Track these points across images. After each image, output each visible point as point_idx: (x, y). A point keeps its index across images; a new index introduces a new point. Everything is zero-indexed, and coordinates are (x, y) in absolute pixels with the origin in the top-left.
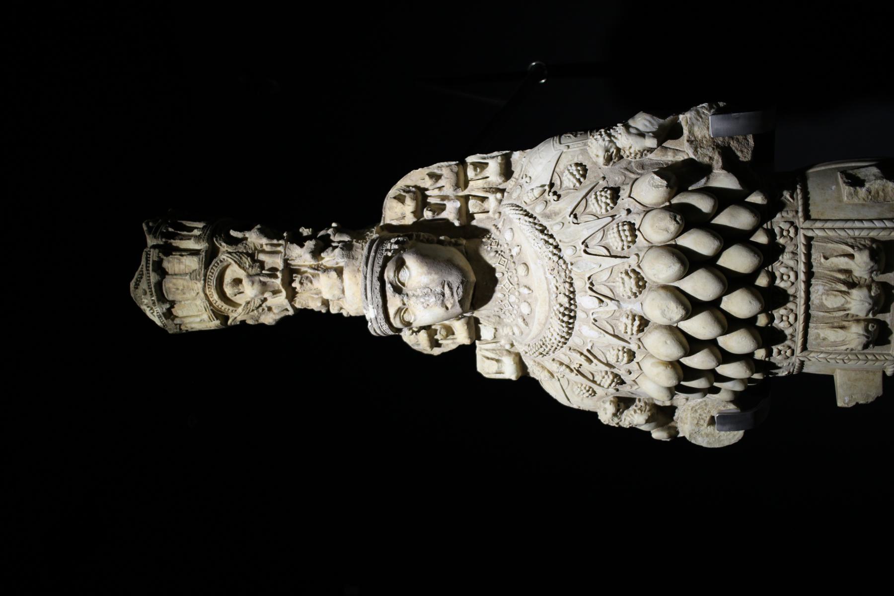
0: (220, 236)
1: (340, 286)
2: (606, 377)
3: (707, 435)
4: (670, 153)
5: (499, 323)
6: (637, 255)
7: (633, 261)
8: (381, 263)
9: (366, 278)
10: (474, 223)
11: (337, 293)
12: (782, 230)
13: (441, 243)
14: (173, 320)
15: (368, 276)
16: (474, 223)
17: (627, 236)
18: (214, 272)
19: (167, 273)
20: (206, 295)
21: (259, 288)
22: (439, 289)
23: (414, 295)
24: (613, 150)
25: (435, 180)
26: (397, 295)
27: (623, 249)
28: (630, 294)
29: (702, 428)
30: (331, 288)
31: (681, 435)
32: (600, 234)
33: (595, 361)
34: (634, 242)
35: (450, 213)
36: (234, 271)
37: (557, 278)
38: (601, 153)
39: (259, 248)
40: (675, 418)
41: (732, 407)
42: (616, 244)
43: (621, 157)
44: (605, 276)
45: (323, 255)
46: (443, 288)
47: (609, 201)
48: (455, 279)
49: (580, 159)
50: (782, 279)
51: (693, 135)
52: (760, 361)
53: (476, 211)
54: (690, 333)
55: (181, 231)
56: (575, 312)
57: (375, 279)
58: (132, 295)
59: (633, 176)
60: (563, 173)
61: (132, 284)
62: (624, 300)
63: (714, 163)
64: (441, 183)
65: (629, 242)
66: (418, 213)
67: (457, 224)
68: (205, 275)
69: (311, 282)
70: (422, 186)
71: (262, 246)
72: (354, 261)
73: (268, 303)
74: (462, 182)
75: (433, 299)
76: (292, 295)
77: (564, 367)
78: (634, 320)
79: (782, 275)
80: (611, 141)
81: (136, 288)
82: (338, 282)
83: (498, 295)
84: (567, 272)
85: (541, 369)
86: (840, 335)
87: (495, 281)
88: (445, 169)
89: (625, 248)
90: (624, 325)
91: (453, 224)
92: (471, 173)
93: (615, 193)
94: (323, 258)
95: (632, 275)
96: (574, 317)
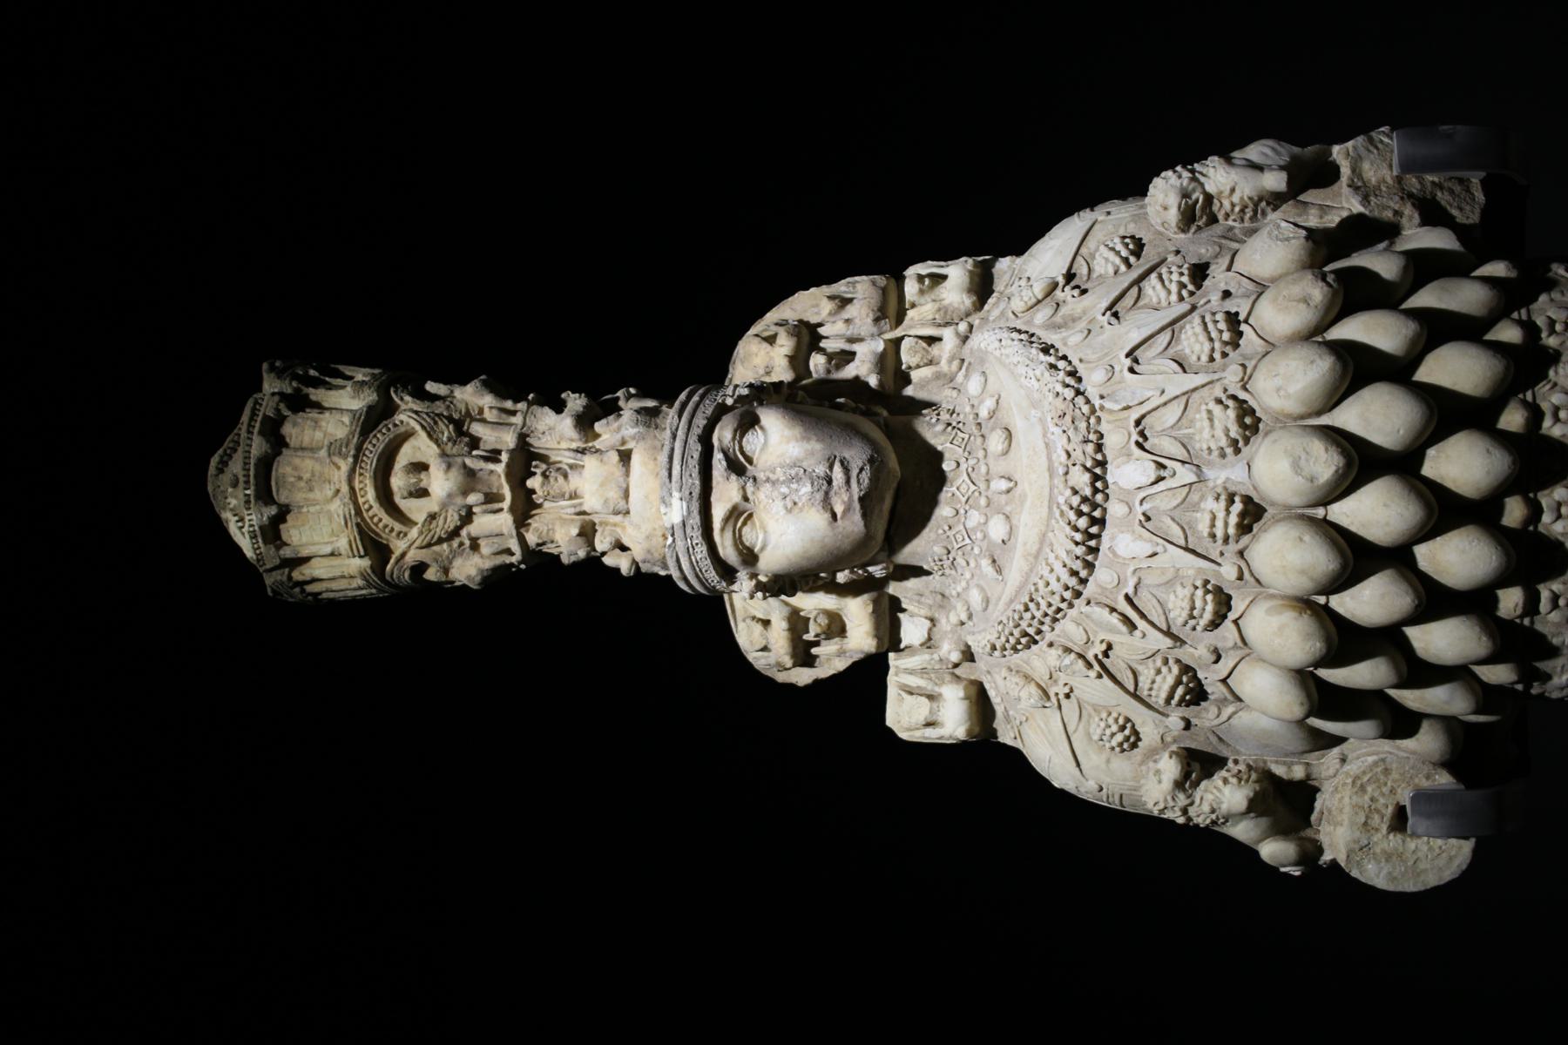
0: (405, 388)
1: (620, 492)
2: (1164, 670)
3: (1388, 857)
4: (1313, 211)
5: (941, 607)
6: (1243, 366)
7: (1231, 377)
8: (709, 412)
9: (674, 436)
10: (909, 391)
11: (614, 494)
12: (1552, 323)
13: (839, 407)
14: (278, 548)
15: (681, 434)
16: (909, 391)
17: (1221, 332)
18: (379, 441)
19: (287, 445)
20: (352, 489)
21: (460, 478)
22: (821, 470)
23: (768, 480)
24: (1198, 195)
25: (842, 317)
26: (734, 477)
27: (1212, 359)
28: (1224, 442)
29: (1376, 837)
30: (602, 485)
31: (1327, 857)
32: (1164, 338)
34: (1236, 346)
35: (862, 368)
36: (420, 447)
37: (1071, 433)
38: (1173, 201)
39: (474, 413)
40: (1313, 817)
41: (1444, 779)
42: (1197, 348)
43: (1213, 220)
44: (1171, 414)
45: (598, 427)
46: (831, 467)
47: (1185, 279)
48: (857, 455)
49: (1132, 229)
50: (1557, 419)
51: (1360, 177)
52: (1511, 623)
53: (913, 361)
54: (1353, 529)
55: (329, 374)
56: (1105, 510)
57: (693, 439)
58: (210, 489)
59: (1235, 245)
60: (1093, 256)
61: (214, 461)
62: (1210, 464)
63: (1404, 221)
64: (851, 311)
65: (1226, 343)
66: (798, 361)
67: (873, 381)
68: (359, 449)
69: (566, 476)
70: (814, 320)
71: (481, 411)
72: (657, 433)
73: (474, 528)
74: (892, 310)
75: (806, 489)
76: (525, 507)
77: (1073, 656)
78: (1231, 501)
79: (1556, 409)
80: (1194, 179)
81: (221, 471)
82: (618, 471)
83: (943, 511)
84: (1092, 420)
85: (1021, 682)
87: (940, 479)
88: (862, 289)
89: (1217, 355)
90: (1213, 515)
91: (866, 384)
92: (911, 288)
93: (1199, 273)
94: (597, 436)
95: (1230, 403)
96: (1101, 522)
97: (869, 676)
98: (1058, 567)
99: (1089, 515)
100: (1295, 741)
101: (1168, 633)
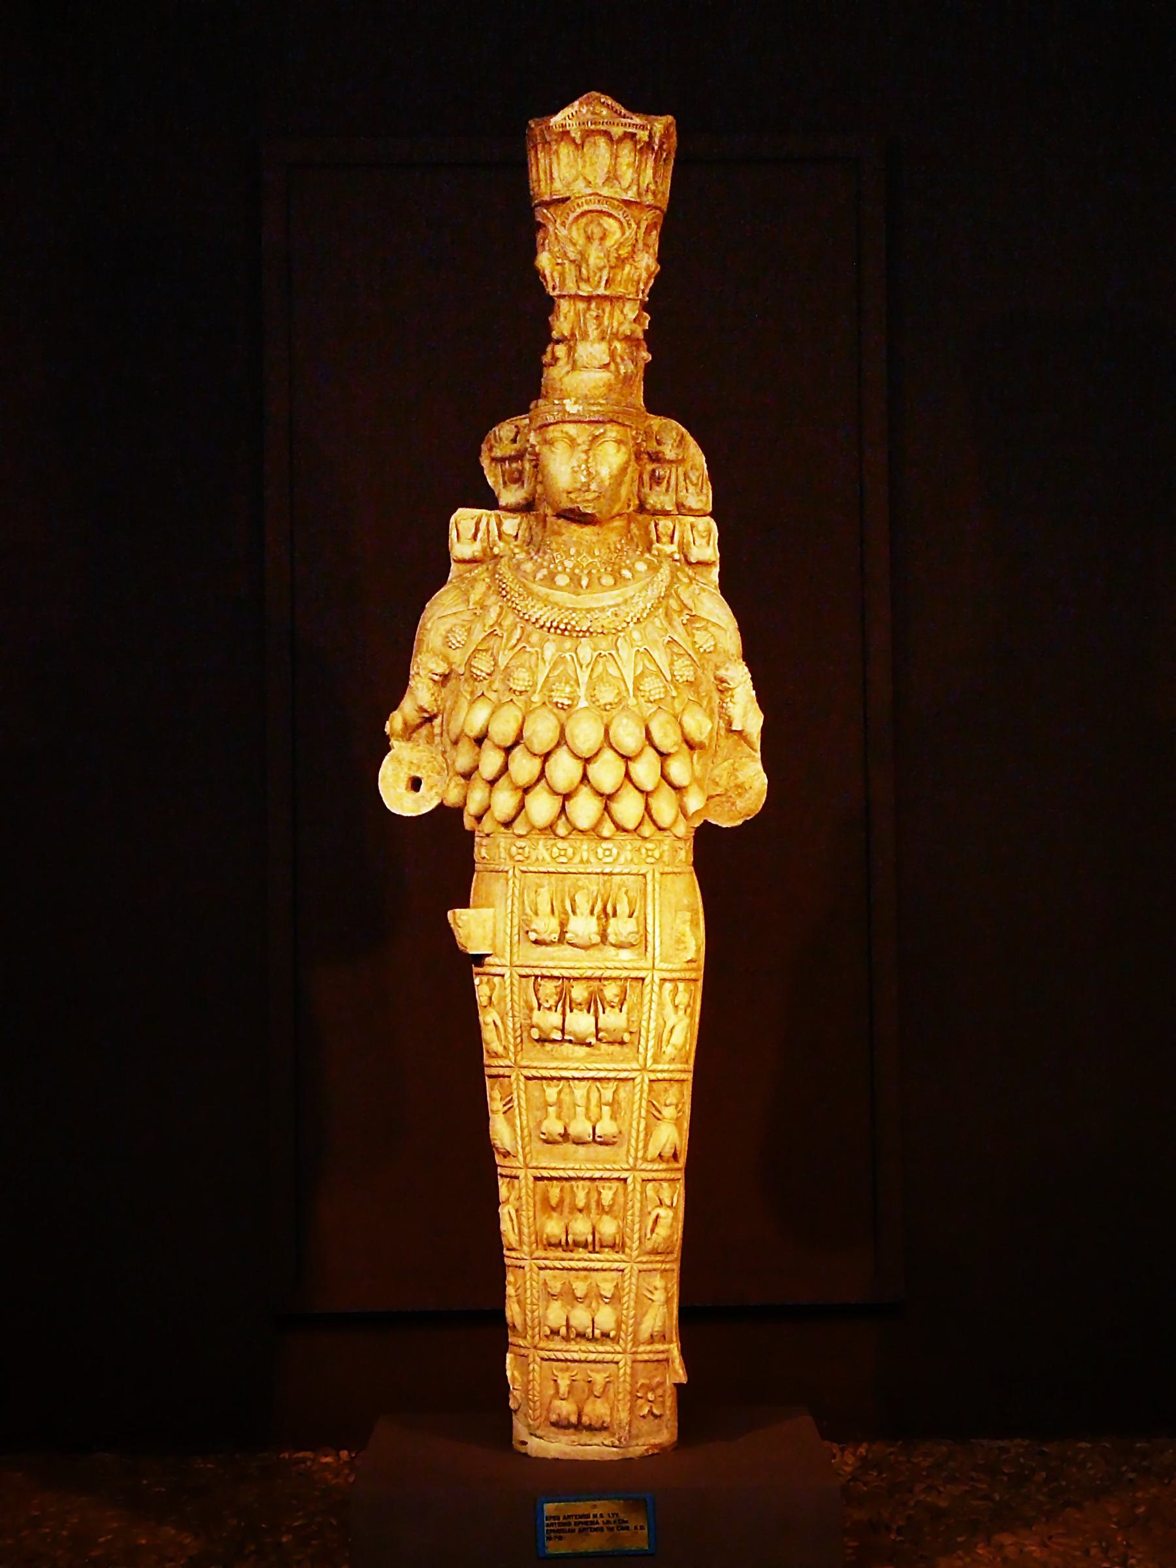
33: (511, 653)
59: (705, 703)
82: (596, 364)
86: (544, 908)
97: (488, 501)
98: (541, 612)
99: (566, 629)
100: (455, 729)
101: (507, 667)
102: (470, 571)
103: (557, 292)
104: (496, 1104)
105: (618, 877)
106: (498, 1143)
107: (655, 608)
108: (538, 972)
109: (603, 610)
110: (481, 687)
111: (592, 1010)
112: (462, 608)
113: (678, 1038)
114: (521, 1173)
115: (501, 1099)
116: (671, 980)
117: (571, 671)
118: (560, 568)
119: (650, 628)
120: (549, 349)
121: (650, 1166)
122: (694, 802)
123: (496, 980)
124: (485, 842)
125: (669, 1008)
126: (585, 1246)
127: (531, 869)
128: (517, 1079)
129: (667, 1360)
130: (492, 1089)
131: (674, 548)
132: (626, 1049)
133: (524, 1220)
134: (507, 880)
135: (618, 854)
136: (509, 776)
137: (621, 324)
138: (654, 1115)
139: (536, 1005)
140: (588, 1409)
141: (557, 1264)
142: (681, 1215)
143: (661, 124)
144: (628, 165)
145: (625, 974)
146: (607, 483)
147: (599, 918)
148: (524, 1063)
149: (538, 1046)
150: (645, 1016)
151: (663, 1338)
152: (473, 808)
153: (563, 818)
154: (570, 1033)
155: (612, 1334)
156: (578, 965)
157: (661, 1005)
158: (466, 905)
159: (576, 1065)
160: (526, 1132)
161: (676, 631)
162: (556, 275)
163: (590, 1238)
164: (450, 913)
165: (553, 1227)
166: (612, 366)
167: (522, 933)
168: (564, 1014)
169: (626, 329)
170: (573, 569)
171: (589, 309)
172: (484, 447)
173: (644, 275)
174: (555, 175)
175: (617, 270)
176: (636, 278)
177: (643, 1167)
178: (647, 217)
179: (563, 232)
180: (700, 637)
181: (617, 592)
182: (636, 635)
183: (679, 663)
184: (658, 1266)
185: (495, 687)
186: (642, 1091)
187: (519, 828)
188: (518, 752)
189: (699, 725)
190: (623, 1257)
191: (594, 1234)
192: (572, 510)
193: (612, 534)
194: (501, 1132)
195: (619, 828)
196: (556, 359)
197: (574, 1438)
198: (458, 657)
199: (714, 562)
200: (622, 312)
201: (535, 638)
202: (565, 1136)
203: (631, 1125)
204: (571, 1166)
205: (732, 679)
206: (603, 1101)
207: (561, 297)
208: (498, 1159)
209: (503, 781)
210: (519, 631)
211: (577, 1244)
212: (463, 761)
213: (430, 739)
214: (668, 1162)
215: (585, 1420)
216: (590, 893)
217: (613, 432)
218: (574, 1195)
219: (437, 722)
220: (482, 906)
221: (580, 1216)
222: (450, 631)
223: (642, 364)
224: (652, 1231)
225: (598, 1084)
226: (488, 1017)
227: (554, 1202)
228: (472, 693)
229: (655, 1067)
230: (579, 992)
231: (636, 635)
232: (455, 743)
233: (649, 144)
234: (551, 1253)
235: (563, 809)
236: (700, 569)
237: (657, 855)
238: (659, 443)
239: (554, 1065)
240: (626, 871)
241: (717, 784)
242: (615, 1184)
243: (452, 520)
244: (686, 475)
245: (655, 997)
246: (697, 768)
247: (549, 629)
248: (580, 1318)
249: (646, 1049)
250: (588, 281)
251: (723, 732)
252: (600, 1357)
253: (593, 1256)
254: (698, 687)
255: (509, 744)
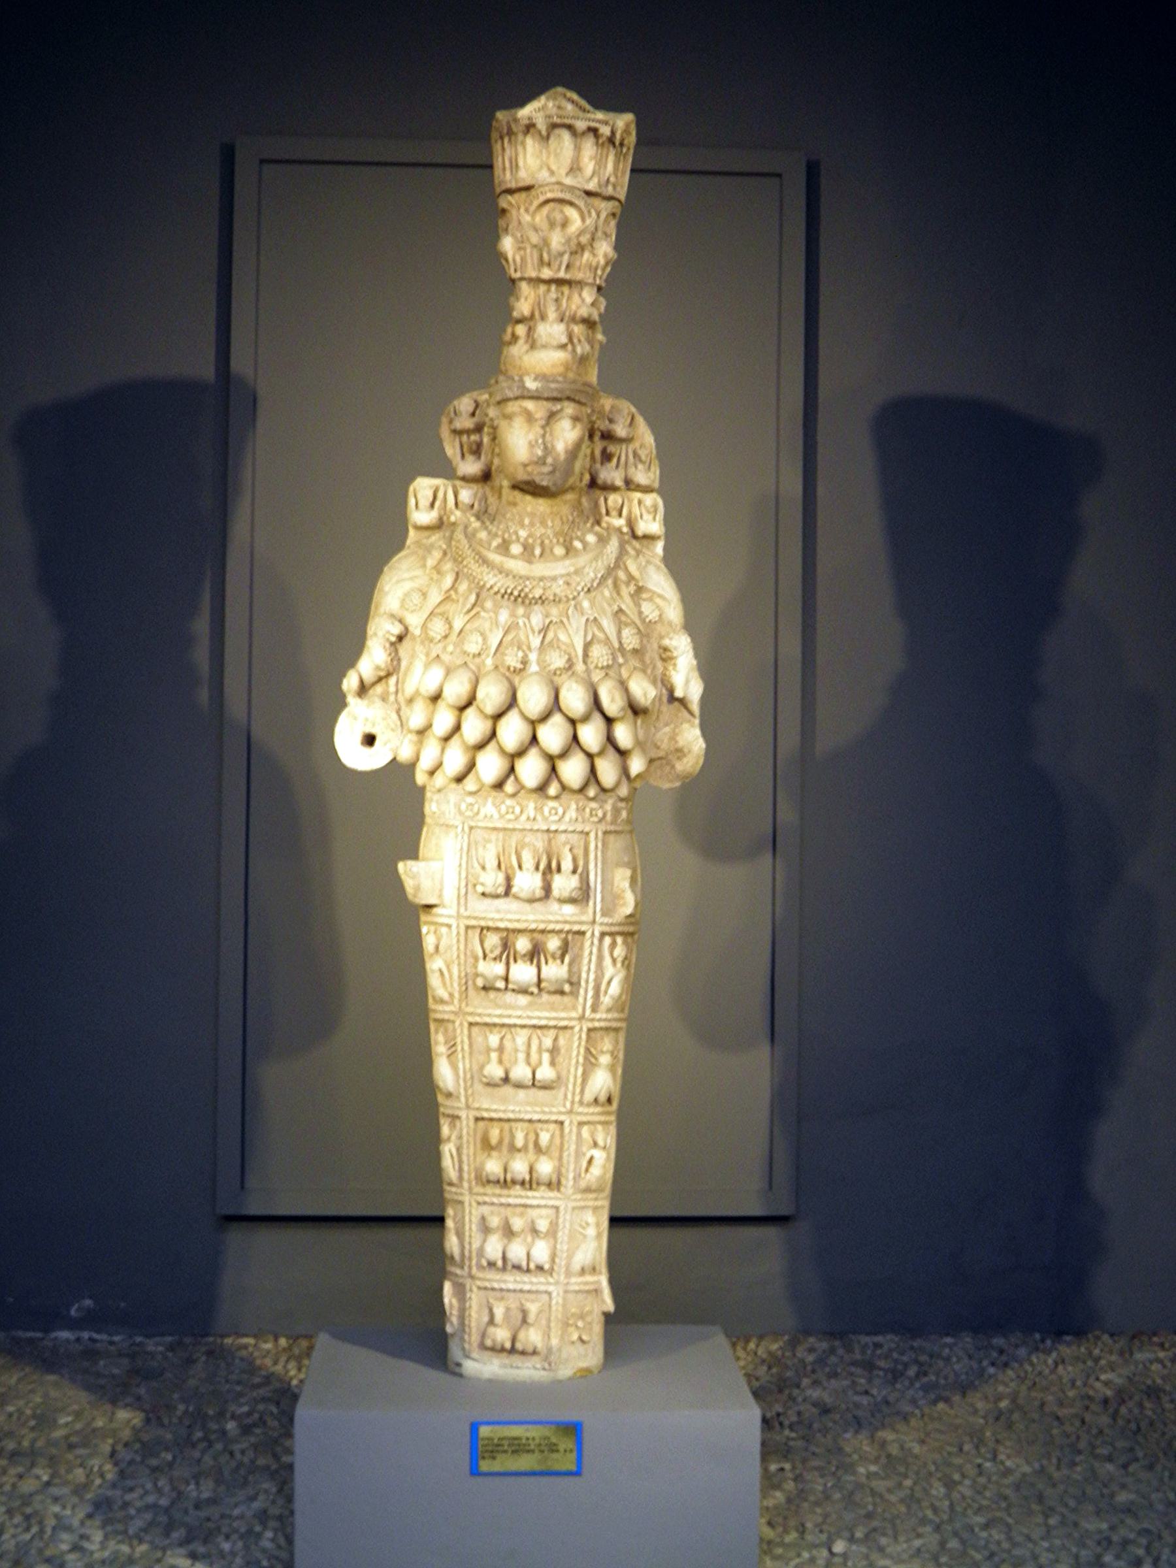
33: (467, 617)
59: (649, 671)
82: (555, 343)
86: (491, 863)
97: (445, 470)
98: (495, 579)
100: (409, 689)
101: (461, 631)
102: (428, 537)
103: (518, 275)
104: (440, 1048)
105: (563, 837)
106: (441, 1084)
107: (603, 579)
108: (483, 923)
109: (554, 579)
110: (436, 650)
111: (535, 962)
112: (419, 572)
113: (615, 989)
114: (463, 1114)
115: (446, 1043)
116: (611, 934)
117: (523, 638)
118: (514, 537)
119: (599, 597)
120: (509, 330)
121: (586, 1110)
122: (636, 765)
123: (444, 930)
124: (436, 797)
125: (608, 961)
126: (523, 1183)
127: (480, 824)
128: (461, 1024)
129: (596, 1291)
130: (437, 1032)
131: (620, 522)
132: (566, 999)
133: (465, 1158)
134: (457, 836)
135: (564, 813)
136: (461, 735)
137: (578, 308)
138: (590, 1063)
139: (480, 954)
140: (522, 1335)
141: (495, 1200)
142: (613, 1156)
143: (623, 121)
144: (591, 159)
145: (567, 927)
146: (562, 457)
147: (544, 874)
148: (470, 1009)
149: (483, 993)
150: (585, 968)
151: (594, 1270)
152: (424, 764)
153: (512, 778)
154: (514, 983)
155: (547, 1267)
156: (524, 918)
157: (600, 958)
158: (414, 855)
159: (519, 1013)
160: (469, 1076)
161: (624, 602)
162: (518, 259)
163: (527, 1178)
164: (401, 866)
165: (493, 1167)
166: (570, 347)
167: (470, 887)
168: (508, 964)
169: (584, 312)
170: (526, 539)
171: (549, 290)
172: (444, 420)
173: (602, 262)
174: (521, 164)
175: (578, 256)
176: (594, 264)
177: (581, 1110)
178: (606, 207)
179: (527, 218)
180: (646, 608)
181: (567, 562)
182: (586, 604)
183: (626, 632)
184: (591, 1203)
185: (450, 648)
186: (580, 1038)
187: (470, 784)
188: (470, 712)
189: (643, 690)
190: (559, 1195)
191: (531, 1172)
192: (528, 483)
193: (564, 506)
194: (444, 1073)
195: (564, 787)
196: (515, 338)
197: (507, 1361)
198: (415, 621)
199: (659, 538)
200: (580, 295)
201: (489, 604)
202: (506, 1080)
203: (569, 1071)
204: (511, 1108)
205: (675, 648)
206: (544, 1047)
207: (522, 279)
208: (440, 1099)
209: (455, 741)
210: (473, 598)
211: (514, 1182)
212: (417, 717)
213: (384, 699)
214: (603, 1105)
215: (519, 1346)
216: (535, 851)
217: (570, 409)
218: (513, 1137)
219: (392, 681)
220: (432, 859)
221: (518, 1155)
222: (407, 595)
223: (597, 346)
224: (587, 1170)
225: (539, 1031)
226: (434, 965)
227: (494, 1141)
228: (427, 655)
229: (593, 1016)
230: (523, 944)
231: (586, 604)
232: (410, 701)
233: (611, 140)
234: (489, 1189)
235: (512, 769)
236: (645, 542)
237: (600, 814)
238: (611, 421)
239: (498, 1012)
240: (571, 829)
241: (658, 748)
242: (552, 1127)
243: (411, 489)
244: (635, 454)
245: (595, 950)
246: (641, 733)
247: (503, 597)
248: (517, 1252)
249: (585, 999)
250: (549, 265)
251: (665, 699)
252: (534, 1288)
253: (530, 1193)
254: (643, 655)
255: (463, 703)
